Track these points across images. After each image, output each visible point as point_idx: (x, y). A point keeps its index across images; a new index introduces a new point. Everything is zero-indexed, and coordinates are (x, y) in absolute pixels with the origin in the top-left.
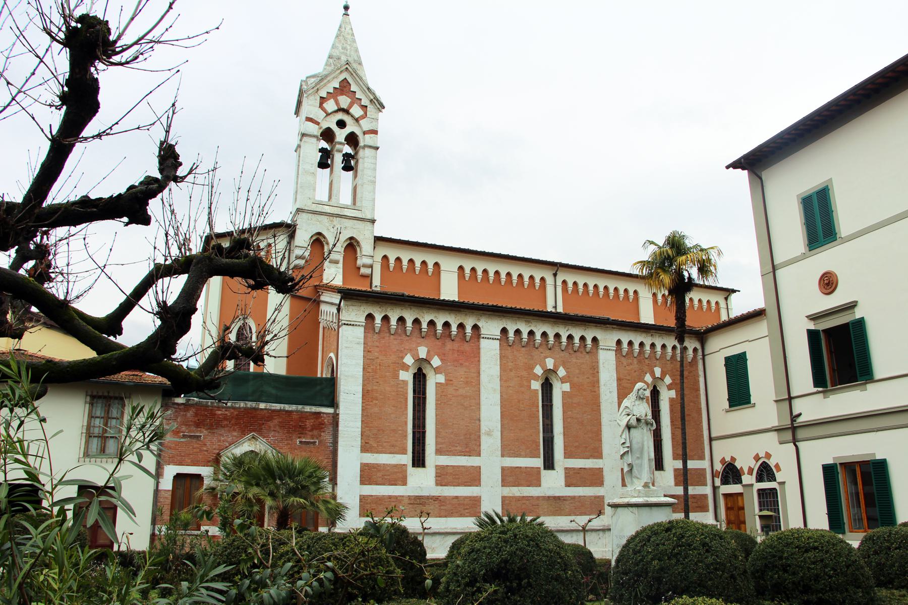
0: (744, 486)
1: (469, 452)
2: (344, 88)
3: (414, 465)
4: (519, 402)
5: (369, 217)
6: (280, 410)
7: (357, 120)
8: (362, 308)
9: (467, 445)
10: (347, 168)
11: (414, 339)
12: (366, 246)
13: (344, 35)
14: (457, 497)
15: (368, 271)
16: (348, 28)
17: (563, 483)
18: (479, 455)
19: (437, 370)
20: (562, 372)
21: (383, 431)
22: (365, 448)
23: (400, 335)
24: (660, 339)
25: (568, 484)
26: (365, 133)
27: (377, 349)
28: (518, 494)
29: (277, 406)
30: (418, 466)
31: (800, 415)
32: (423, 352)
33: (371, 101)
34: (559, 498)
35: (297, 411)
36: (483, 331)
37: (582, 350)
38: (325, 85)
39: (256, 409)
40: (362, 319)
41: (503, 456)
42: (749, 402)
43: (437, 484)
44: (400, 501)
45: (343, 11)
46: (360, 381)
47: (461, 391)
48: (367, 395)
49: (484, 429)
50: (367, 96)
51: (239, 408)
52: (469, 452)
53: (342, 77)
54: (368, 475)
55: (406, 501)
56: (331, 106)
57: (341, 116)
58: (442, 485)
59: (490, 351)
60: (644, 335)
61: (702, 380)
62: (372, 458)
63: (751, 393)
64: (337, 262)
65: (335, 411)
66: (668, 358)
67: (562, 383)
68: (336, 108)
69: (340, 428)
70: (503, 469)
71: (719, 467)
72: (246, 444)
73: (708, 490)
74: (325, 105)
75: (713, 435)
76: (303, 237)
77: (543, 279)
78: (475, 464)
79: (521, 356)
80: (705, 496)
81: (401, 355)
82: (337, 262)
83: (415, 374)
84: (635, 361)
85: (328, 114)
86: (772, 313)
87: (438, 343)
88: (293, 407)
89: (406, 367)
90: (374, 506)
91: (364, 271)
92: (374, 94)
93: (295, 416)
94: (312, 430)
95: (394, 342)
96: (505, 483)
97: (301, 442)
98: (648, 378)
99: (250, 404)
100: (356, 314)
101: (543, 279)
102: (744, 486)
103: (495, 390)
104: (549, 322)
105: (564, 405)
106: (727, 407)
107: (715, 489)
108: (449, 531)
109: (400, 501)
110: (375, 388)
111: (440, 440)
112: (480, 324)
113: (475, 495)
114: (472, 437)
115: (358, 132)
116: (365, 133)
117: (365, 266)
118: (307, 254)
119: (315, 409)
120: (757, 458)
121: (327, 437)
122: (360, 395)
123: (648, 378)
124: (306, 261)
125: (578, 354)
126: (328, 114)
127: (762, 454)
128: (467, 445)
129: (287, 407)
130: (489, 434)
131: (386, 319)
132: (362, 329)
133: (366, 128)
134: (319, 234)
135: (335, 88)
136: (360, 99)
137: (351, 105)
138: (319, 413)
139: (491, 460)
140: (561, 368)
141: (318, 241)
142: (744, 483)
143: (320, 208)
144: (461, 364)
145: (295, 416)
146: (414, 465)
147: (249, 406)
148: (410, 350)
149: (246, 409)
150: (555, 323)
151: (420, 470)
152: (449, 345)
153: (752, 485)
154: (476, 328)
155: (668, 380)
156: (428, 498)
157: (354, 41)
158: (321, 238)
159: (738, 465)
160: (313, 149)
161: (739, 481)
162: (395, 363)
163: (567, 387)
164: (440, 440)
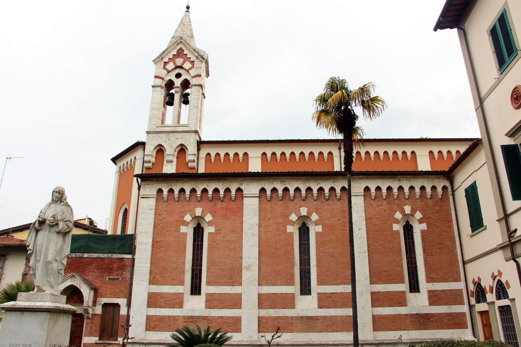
0: (489, 304)
1: (233, 282)
2: (180, 53)
3: (192, 293)
4: (276, 242)
5: (193, 129)
6: (97, 258)
7: (188, 71)
8: (154, 186)
9: (231, 278)
10: (186, 102)
11: (192, 203)
12: (192, 149)
13: (185, 23)
14: (222, 317)
15: (195, 165)
16: (187, 20)
17: (316, 305)
18: (241, 285)
19: (210, 223)
20: (314, 217)
21: (167, 269)
22: (152, 282)
23: (182, 201)
24: (408, 182)
25: (320, 307)
26: (193, 77)
27: (165, 213)
28: (274, 315)
29: (95, 255)
30: (196, 294)
31: (516, 230)
32: (198, 212)
33: (197, 57)
34: (312, 318)
35: (108, 258)
37: (333, 198)
38: (167, 54)
39: (82, 258)
40: (154, 192)
42: (482, 226)
43: (206, 307)
44: (177, 320)
45: (186, 10)
46: (151, 235)
47: (228, 238)
48: (155, 244)
49: (244, 264)
50: (194, 55)
51: (72, 257)
52: (233, 282)
53: (178, 48)
54: (153, 300)
55: (182, 320)
56: (171, 66)
57: (178, 71)
58: (210, 308)
59: (251, 206)
60: (391, 180)
61: (453, 212)
62: (156, 289)
63: (483, 218)
64: (171, 162)
65: (133, 257)
66: (418, 197)
67: (316, 225)
68: (174, 66)
69: (135, 268)
70: (260, 295)
71: (472, 287)
72: (69, 281)
73: (464, 309)
74: (167, 67)
75: (466, 258)
76: (150, 149)
77: (330, 153)
78: (237, 292)
79: (278, 207)
80: (463, 314)
81: (182, 215)
82: (171, 162)
83: (195, 229)
84: (385, 202)
85: (169, 72)
86: (485, 141)
87: (211, 204)
88: (106, 256)
89: (186, 224)
90: (157, 323)
91: (190, 165)
92: (198, 52)
93: (106, 261)
94: (117, 270)
95: (178, 207)
96: (261, 306)
97: (109, 279)
98: (398, 215)
100: (151, 190)
101: (330, 153)
102: (489, 304)
103: (254, 235)
104: (301, 180)
105: (317, 242)
106: (470, 232)
107: (471, 307)
108: (153, 342)
109: (177, 320)
110: (163, 239)
111: (209, 274)
113: (237, 315)
114: (236, 271)
115: (188, 78)
116: (193, 77)
117: (190, 161)
118: (153, 160)
120: (494, 278)
121: (127, 275)
122: (150, 245)
123: (398, 215)
124: (153, 164)
125: (329, 202)
126: (169, 72)
127: (496, 274)
128: (231, 278)
129: (102, 256)
130: (248, 268)
131: (171, 191)
132: (154, 200)
133: (193, 75)
134: (161, 145)
135: (174, 55)
136: (190, 58)
137: (183, 63)
138: (123, 259)
140: (314, 214)
141: (160, 150)
142: (488, 301)
143: (158, 129)
144: (228, 218)
145: (106, 261)
146: (192, 293)
147: (77, 256)
148: (189, 211)
149: (76, 258)
150: (307, 180)
152: (219, 205)
153: (493, 303)
154: (239, 190)
155: (418, 215)
156: (198, 317)
157: (190, 25)
158: (162, 148)
159: (483, 284)
160: (161, 94)
161: (484, 300)
162: (177, 221)
164: (209, 274)
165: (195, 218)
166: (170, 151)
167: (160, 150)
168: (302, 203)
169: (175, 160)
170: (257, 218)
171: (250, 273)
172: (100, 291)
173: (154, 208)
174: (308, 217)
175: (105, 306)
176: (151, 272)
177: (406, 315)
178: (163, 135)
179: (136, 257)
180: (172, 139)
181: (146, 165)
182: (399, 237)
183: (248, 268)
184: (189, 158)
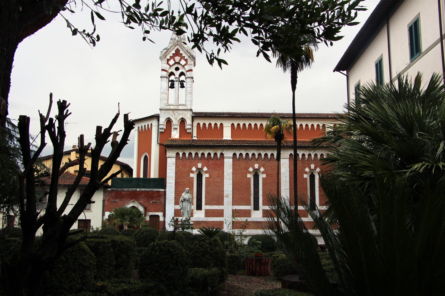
2: (177, 53)
3: (197, 209)
5: (189, 108)
10: (182, 86)
14: (213, 221)
15: (190, 131)
17: (262, 216)
18: (223, 205)
19: (206, 172)
29: (143, 189)
32: (200, 166)
34: (259, 222)
35: (151, 191)
36: (225, 155)
38: (169, 53)
39: (136, 191)
40: (175, 155)
41: (233, 205)
43: (205, 217)
47: (216, 180)
49: (225, 194)
50: (187, 55)
53: (176, 48)
56: (172, 62)
57: (176, 66)
59: (228, 163)
60: (305, 150)
64: (177, 129)
68: (174, 63)
70: (233, 210)
74: (169, 62)
76: (162, 120)
82: (177, 129)
85: (171, 66)
87: (206, 161)
89: (193, 172)
91: (188, 131)
94: (156, 197)
98: (307, 170)
99: (135, 189)
104: (255, 149)
105: (263, 183)
112: (223, 153)
114: (221, 198)
117: (188, 129)
118: (165, 127)
119: (157, 190)
122: (174, 184)
125: (271, 161)
126: (171, 66)
129: (147, 190)
130: (227, 196)
131: (184, 154)
132: (175, 159)
133: (187, 70)
134: (169, 118)
137: (180, 60)
139: (228, 207)
140: (262, 168)
141: (169, 121)
144: (216, 169)
146: (197, 209)
151: (199, 211)
152: (211, 162)
154: (222, 154)
155: (318, 170)
163: (264, 176)
165: (197, 169)
166: (175, 123)
167: (169, 121)
168: (256, 161)
169: (178, 127)
170: (231, 170)
171: (228, 199)
172: (148, 209)
173: (175, 163)
174: (259, 169)
175: (151, 216)
176: (175, 198)
177: (307, 222)
178: (171, 112)
179: (167, 190)
180: (176, 114)
181: (160, 130)
182: (307, 181)
183: (227, 196)
184: (187, 127)
